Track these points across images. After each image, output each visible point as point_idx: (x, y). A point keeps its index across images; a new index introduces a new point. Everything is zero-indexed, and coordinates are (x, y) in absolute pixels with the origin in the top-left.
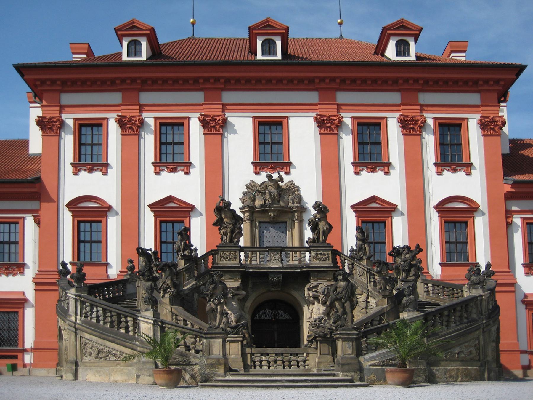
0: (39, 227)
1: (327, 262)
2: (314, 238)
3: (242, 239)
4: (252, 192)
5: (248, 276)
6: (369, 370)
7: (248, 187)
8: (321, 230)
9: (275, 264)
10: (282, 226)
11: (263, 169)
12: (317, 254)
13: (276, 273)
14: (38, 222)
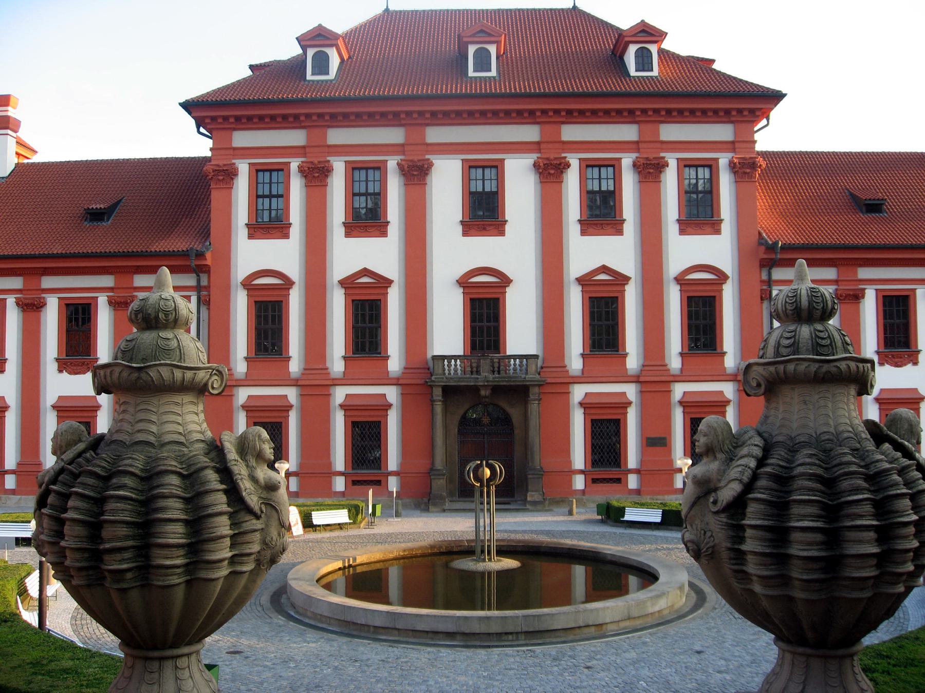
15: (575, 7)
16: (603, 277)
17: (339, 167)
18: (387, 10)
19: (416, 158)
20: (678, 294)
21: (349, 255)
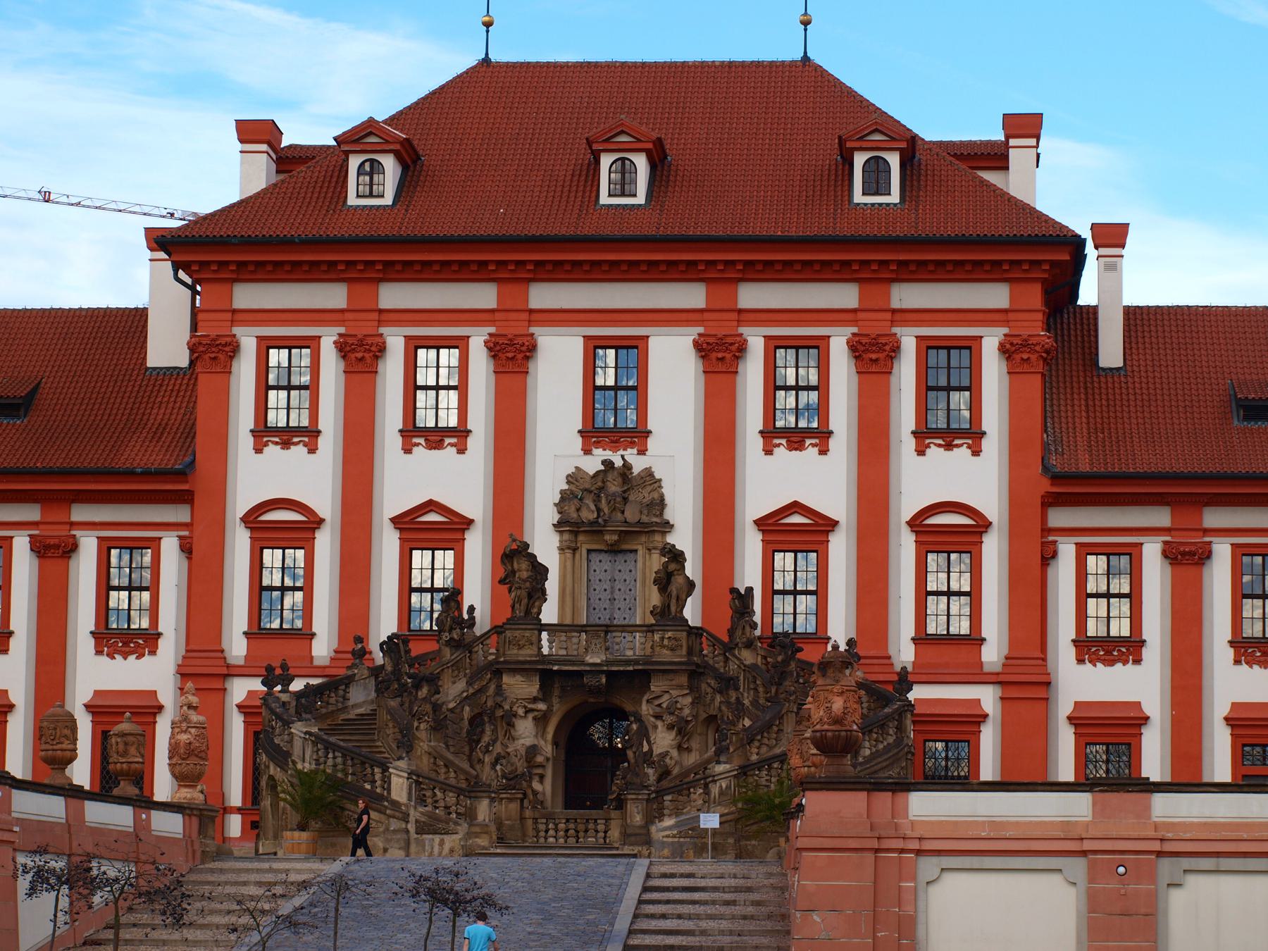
0: (189, 558)
1: (678, 652)
2: (663, 605)
3: (545, 607)
4: (577, 491)
5: (551, 677)
6: (663, 843)
7: (568, 482)
8: (674, 594)
9: (594, 659)
10: (630, 557)
11: (598, 444)
12: (662, 639)
13: (596, 670)
14: (186, 548)
15: (806, 58)
16: (797, 519)
17: (395, 342)
18: (486, 61)
19: (511, 331)
20: (913, 546)
21: (406, 479)
